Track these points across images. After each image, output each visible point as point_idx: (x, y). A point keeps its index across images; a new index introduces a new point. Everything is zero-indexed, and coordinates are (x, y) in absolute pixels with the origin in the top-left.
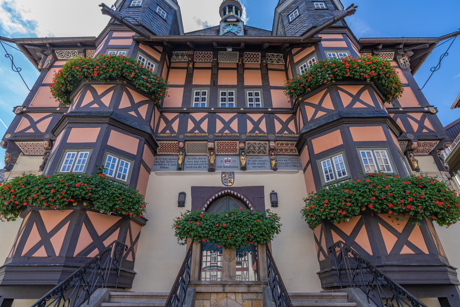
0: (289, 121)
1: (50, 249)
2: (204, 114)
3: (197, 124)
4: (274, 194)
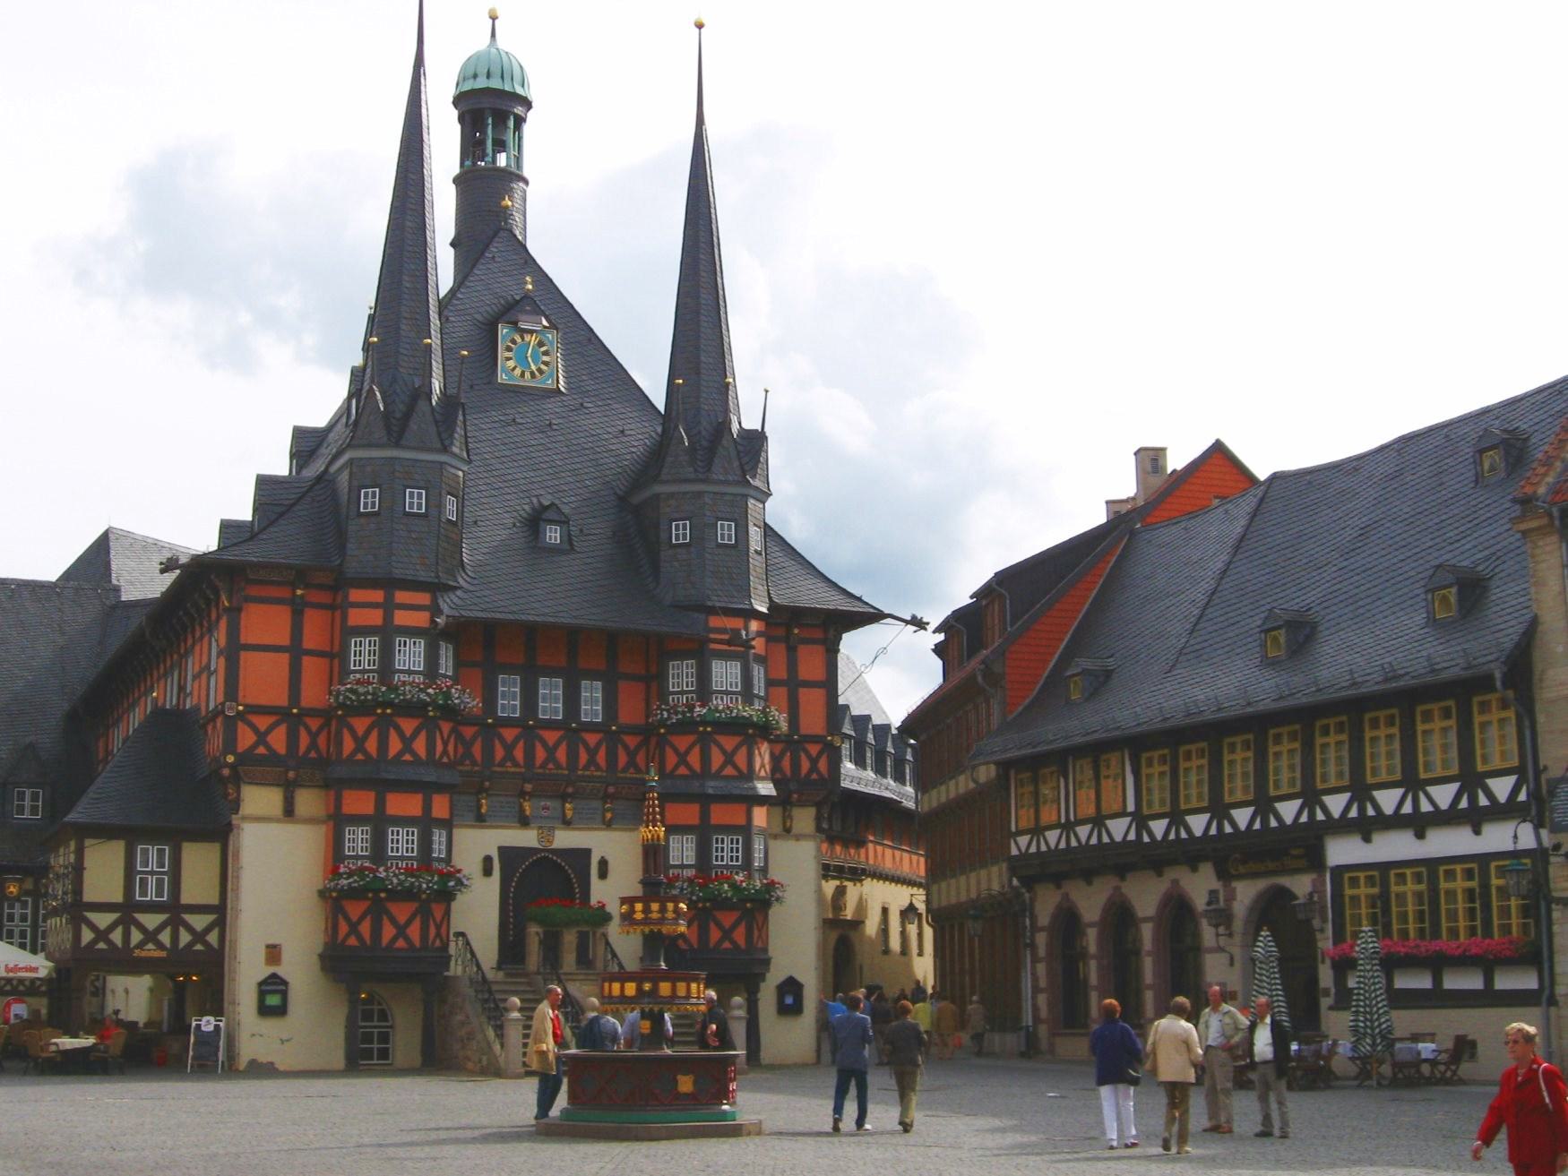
1: (407, 938)
2: (516, 731)
3: (509, 748)
4: (603, 864)
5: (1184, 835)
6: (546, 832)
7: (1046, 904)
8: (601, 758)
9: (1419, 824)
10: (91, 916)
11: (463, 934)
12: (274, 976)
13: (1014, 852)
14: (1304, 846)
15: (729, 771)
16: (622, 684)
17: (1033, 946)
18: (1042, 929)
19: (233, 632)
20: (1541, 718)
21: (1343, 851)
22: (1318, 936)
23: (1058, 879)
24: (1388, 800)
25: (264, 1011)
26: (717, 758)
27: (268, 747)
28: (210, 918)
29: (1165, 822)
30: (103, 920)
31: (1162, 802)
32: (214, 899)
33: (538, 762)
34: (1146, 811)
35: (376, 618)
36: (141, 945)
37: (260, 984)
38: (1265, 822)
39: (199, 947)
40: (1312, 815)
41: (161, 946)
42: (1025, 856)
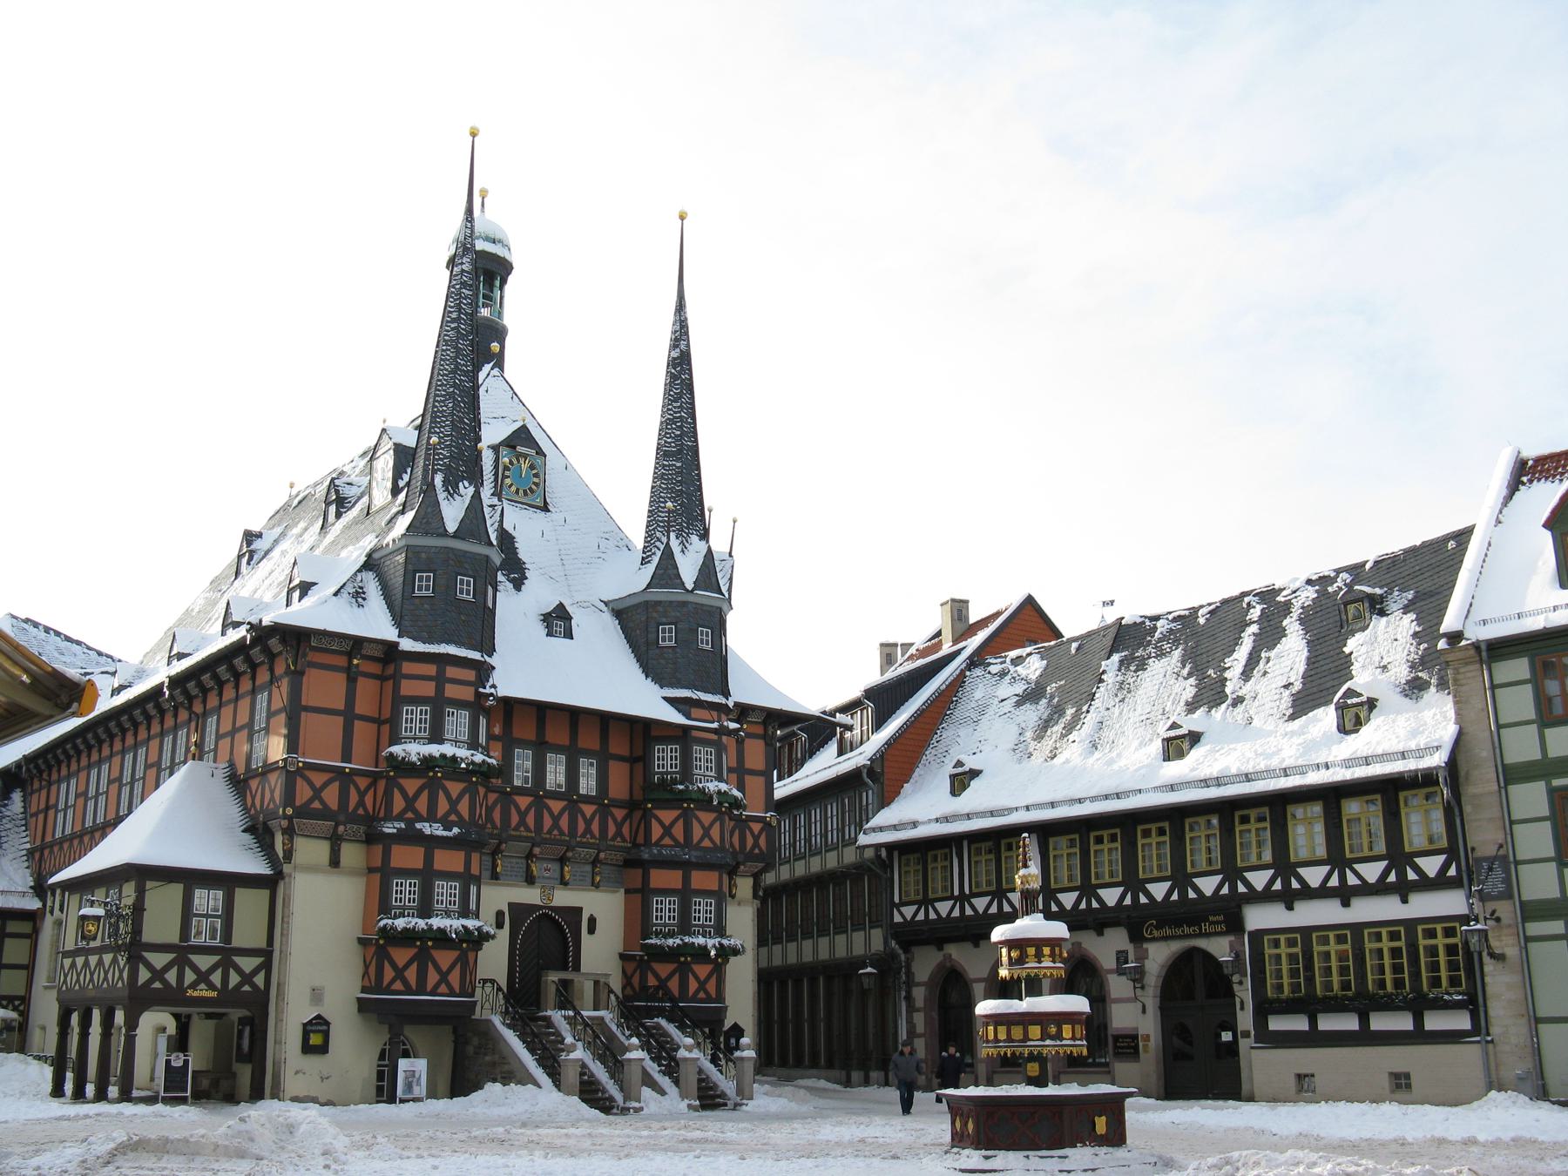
0: (624, 820)
2: (530, 799)
3: (523, 815)
4: (592, 921)
5: (1095, 905)
6: (547, 891)
7: (925, 964)
8: (595, 827)
9: (1345, 895)
10: (149, 956)
11: (493, 981)
12: (319, 1017)
13: (897, 919)
14: (1228, 914)
15: (706, 843)
16: (611, 763)
17: (909, 998)
18: (918, 984)
19: (295, 693)
20: (1467, 809)
21: (1259, 918)
22: (1236, 987)
23: (940, 943)
24: (1314, 876)
25: (307, 1049)
26: (697, 832)
27: (322, 802)
28: (257, 961)
29: (1074, 895)
30: (159, 960)
31: (989, 883)
32: (262, 944)
33: (545, 830)
34: (1053, 886)
35: (428, 689)
36: (193, 986)
37: (305, 1025)
38: (1183, 894)
39: (247, 988)
40: (1233, 888)
41: (212, 987)
42: (910, 924)
